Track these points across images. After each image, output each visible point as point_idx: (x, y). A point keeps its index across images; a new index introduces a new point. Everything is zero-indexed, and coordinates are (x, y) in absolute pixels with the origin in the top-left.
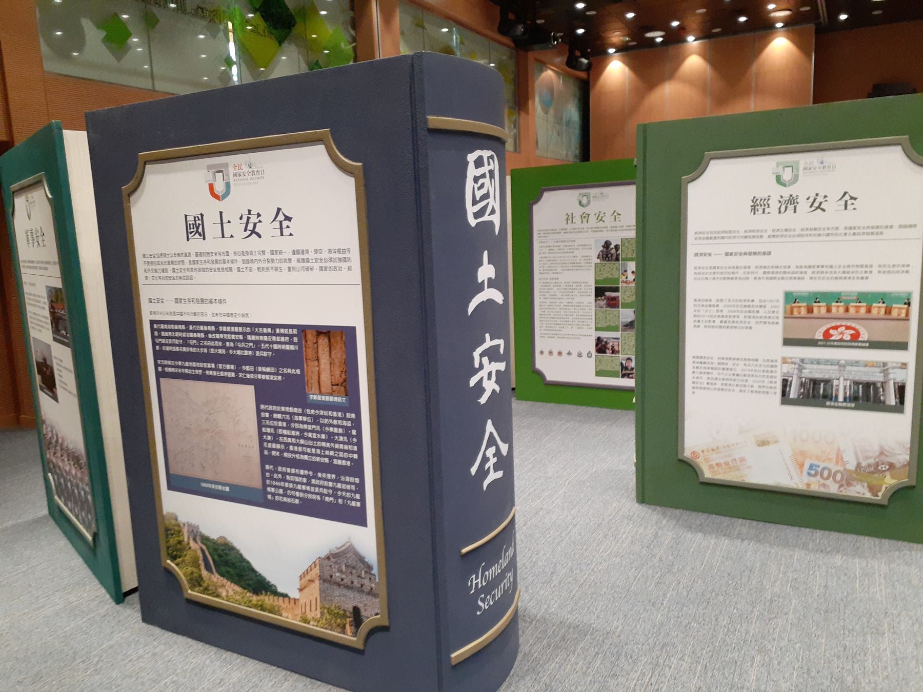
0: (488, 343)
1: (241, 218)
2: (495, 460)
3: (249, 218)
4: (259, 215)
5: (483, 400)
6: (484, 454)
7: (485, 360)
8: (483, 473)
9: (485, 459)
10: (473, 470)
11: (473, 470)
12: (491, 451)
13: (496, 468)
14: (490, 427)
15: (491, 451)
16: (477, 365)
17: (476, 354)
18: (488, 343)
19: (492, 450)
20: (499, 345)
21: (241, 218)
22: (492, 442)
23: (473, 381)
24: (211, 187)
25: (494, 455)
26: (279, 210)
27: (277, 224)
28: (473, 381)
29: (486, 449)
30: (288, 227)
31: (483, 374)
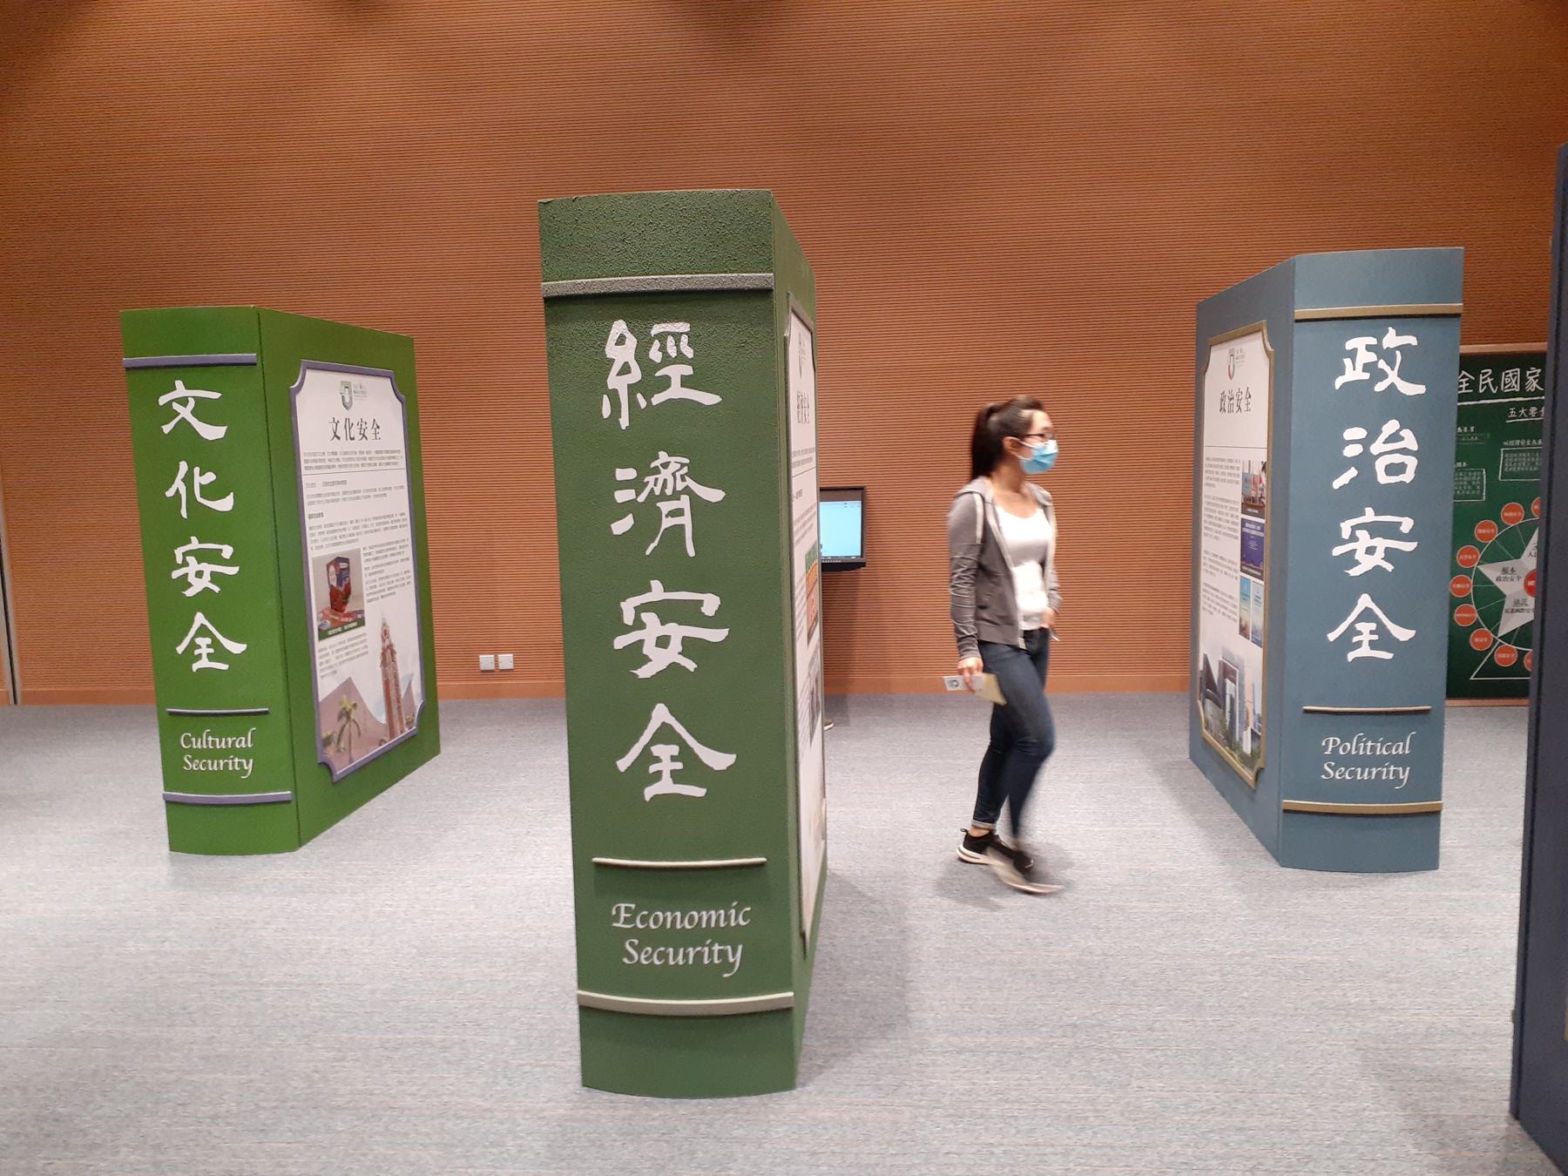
6: (647, 748)
7: (650, 618)
9: (647, 757)
10: (623, 764)
11: (623, 764)
13: (677, 777)
15: (665, 752)
16: (629, 618)
17: (628, 608)
18: (657, 592)
19: (674, 750)
20: (701, 602)
22: (665, 735)
23: (620, 642)
25: (673, 759)
28: (620, 642)
29: (655, 740)
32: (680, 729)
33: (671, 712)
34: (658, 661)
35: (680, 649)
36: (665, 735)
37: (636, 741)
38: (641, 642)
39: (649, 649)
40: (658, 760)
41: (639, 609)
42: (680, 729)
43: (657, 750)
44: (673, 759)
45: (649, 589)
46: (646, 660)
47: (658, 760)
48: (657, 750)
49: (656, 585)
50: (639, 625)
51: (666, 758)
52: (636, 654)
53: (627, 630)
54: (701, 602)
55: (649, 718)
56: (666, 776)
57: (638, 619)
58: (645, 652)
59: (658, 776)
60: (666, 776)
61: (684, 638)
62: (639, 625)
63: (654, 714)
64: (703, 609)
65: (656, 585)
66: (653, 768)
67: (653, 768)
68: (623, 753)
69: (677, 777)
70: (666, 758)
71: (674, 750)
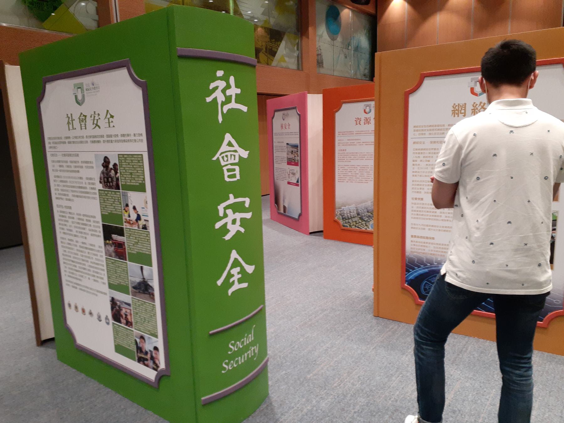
0: (232, 200)
1: (91, 117)
2: (240, 276)
3: (94, 117)
4: (99, 115)
5: (228, 237)
7: (229, 212)
8: (228, 284)
9: (230, 276)
10: (219, 282)
11: (219, 282)
12: (235, 271)
13: (240, 281)
14: (234, 255)
15: (235, 271)
16: (221, 214)
17: (221, 208)
18: (232, 200)
19: (238, 269)
20: (244, 202)
21: (91, 117)
22: (236, 263)
23: (218, 225)
24: (76, 97)
25: (239, 273)
26: (108, 111)
27: (107, 120)
28: (218, 225)
29: (232, 268)
30: (112, 122)
31: (229, 220)
32: (240, 259)
33: (238, 253)
34: (233, 229)
36: (236, 263)
37: (225, 269)
38: (226, 223)
39: (230, 226)
40: (233, 276)
41: (226, 208)
42: (240, 259)
44: (239, 273)
45: (228, 198)
46: (228, 231)
47: (233, 276)
49: (231, 196)
50: (225, 215)
51: (236, 274)
52: (224, 230)
53: (220, 219)
54: (244, 202)
55: (230, 257)
56: (236, 282)
58: (228, 228)
60: (236, 282)
61: (241, 219)
62: (225, 215)
65: (231, 196)
66: (231, 280)
67: (231, 280)
69: (240, 281)
70: (236, 274)
71: (238, 269)
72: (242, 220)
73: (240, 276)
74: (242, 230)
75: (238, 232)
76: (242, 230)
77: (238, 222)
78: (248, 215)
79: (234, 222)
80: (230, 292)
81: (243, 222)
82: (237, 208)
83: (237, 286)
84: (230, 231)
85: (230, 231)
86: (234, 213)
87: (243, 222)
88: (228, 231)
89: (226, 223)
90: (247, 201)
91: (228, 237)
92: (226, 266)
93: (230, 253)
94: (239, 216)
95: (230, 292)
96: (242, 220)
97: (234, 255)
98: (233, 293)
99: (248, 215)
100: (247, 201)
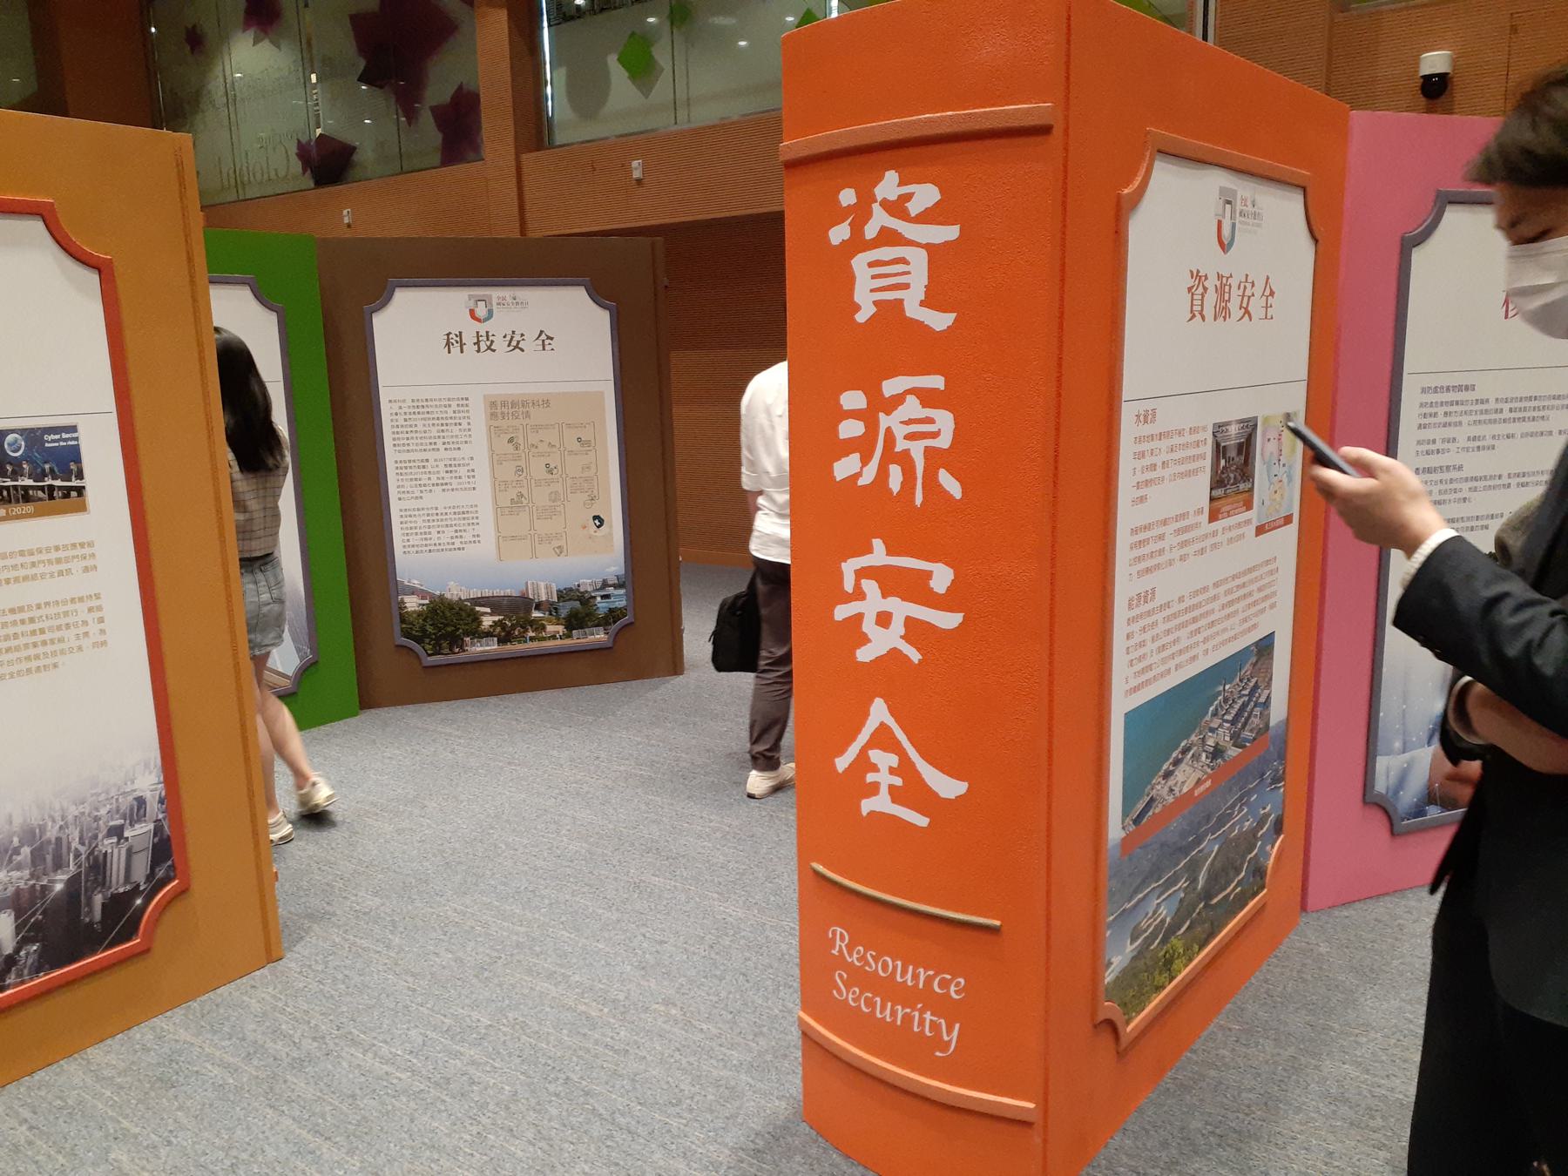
2: (898, 781)
5: (865, 655)
6: (863, 752)
7: (870, 586)
9: (863, 764)
12: (884, 760)
14: (879, 713)
16: (849, 585)
17: (849, 567)
18: (879, 555)
19: (893, 760)
20: (929, 574)
22: (883, 739)
23: (842, 612)
25: (892, 771)
28: (842, 612)
29: (870, 744)
34: (879, 643)
35: (902, 631)
36: (883, 739)
37: (854, 739)
38: (859, 618)
39: (869, 626)
40: (875, 768)
41: (861, 573)
43: (875, 755)
44: (892, 771)
46: (864, 640)
47: (875, 768)
48: (875, 755)
49: (878, 544)
50: (859, 595)
52: (853, 631)
53: (848, 598)
55: (866, 714)
57: (857, 585)
58: (865, 629)
59: (874, 789)
60: (884, 790)
61: (908, 618)
62: (859, 595)
63: (873, 709)
64: (932, 584)
65: (878, 544)
66: (870, 777)
67: (870, 777)
68: (841, 752)
69: (896, 795)
71: (893, 760)
72: (910, 622)
73: (898, 781)
74: (915, 656)
75: (894, 652)
76: (915, 656)
77: (898, 627)
78: (948, 620)
79: (884, 619)
80: (867, 806)
81: (915, 630)
82: (891, 581)
83: (881, 803)
84: (869, 641)
85: (869, 641)
86: (884, 596)
87: (915, 630)
88: (864, 640)
89: (859, 618)
90: (942, 578)
91: (865, 655)
92: (859, 731)
93: (871, 701)
94: (902, 609)
95: (867, 806)
96: (910, 622)
97: (879, 713)
98: (872, 813)
99: (948, 620)
100: (942, 578)
